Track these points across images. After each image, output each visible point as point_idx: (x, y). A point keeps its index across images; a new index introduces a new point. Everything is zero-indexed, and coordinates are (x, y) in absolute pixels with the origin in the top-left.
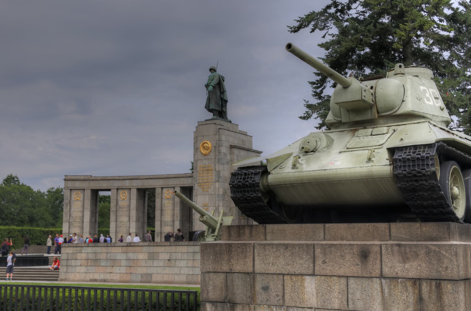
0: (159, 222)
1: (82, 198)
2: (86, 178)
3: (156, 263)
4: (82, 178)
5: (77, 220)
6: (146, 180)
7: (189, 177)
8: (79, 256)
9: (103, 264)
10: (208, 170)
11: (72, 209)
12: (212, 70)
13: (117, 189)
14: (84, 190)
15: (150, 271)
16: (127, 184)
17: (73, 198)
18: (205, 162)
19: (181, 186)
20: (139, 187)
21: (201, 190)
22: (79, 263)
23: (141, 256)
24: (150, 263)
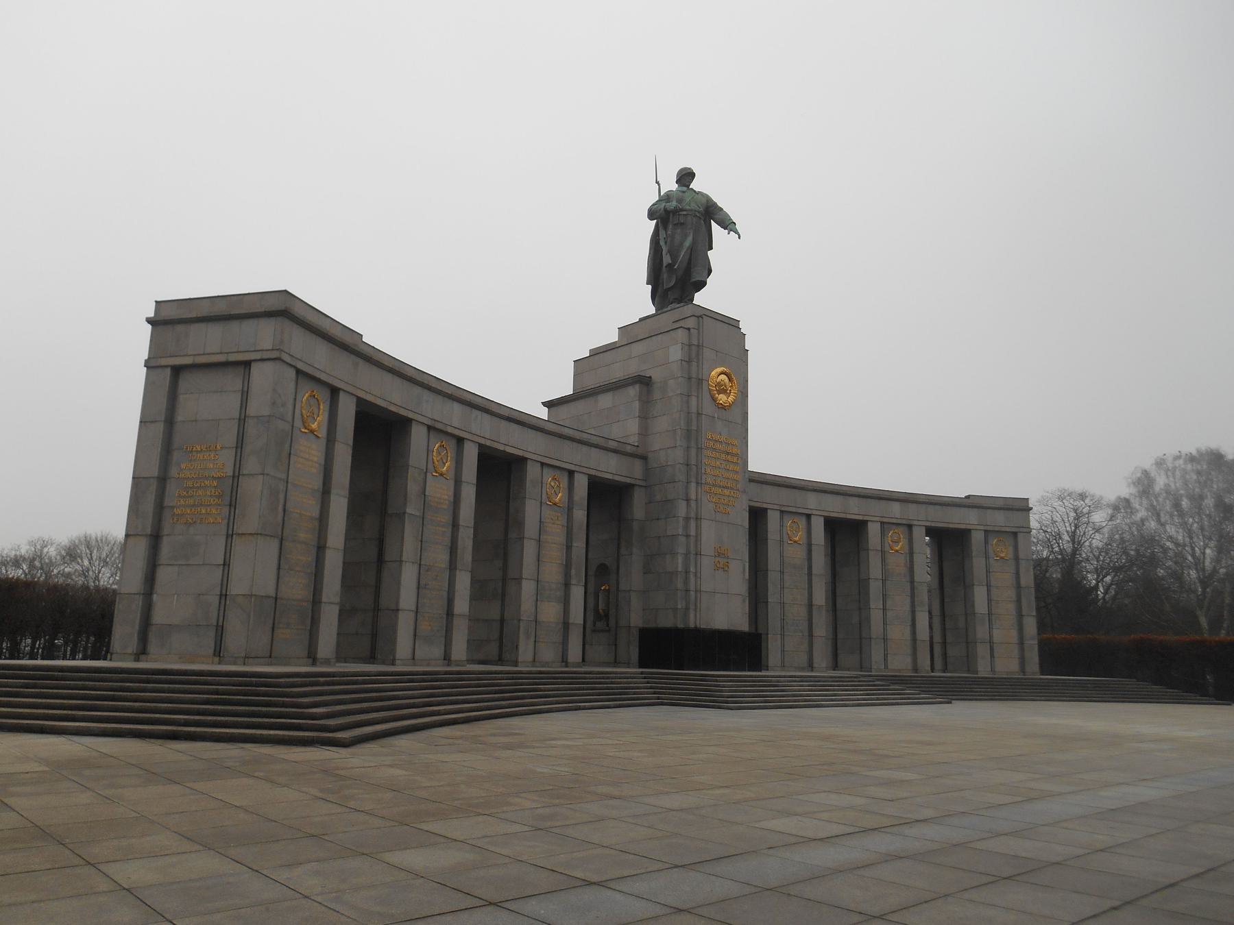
0: (533, 585)
1: (323, 433)
2: (348, 339)
4: (337, 333)
5: (302, 536)
6: (504, 423)
7: (615, 451)
10: (728, 454)
12: (686, 177)
13: (430, 428)
16: (454, 417)
17: (298, 423)
19: (593, 473)
20: (488, 443)
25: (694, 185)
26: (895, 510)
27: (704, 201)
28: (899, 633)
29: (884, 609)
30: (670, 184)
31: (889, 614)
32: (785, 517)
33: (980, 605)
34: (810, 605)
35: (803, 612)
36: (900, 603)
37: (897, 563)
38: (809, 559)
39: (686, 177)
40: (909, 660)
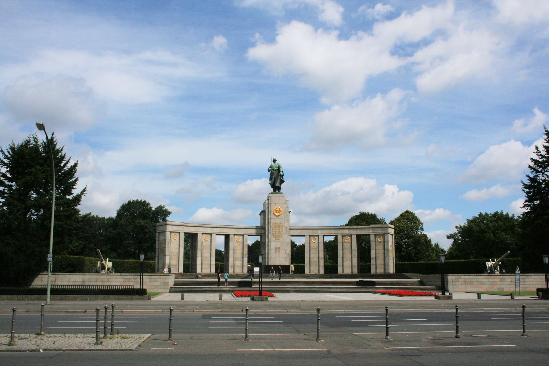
2: (181, 224)
3: (505, 283)
8: (460, 280)
9: (475, 283)
11: (172, 247)
12: (274, 161)
13: (202, 234)
14: (179, 233)
15: (502, 286)
16: (209, 230)
17: (172, 239)
18: (277, 220)
21: (274, 239)
22: (460, 283)
23: (496, 280)
24: (501, 283)
25: (277, 162)
26: (346, 232)
27: (277, 166)
28: (347, 263)
29: (343, 258)
30: (271, 163)
31: (344, 259)
32: (312, 238)
33: (373, 254)
34: (319, 258)
35: (317, 259)
36: (348, 255)
37: (347, 246)
38: (319, 246)
39: (274, 161)
40: (350, 270)
